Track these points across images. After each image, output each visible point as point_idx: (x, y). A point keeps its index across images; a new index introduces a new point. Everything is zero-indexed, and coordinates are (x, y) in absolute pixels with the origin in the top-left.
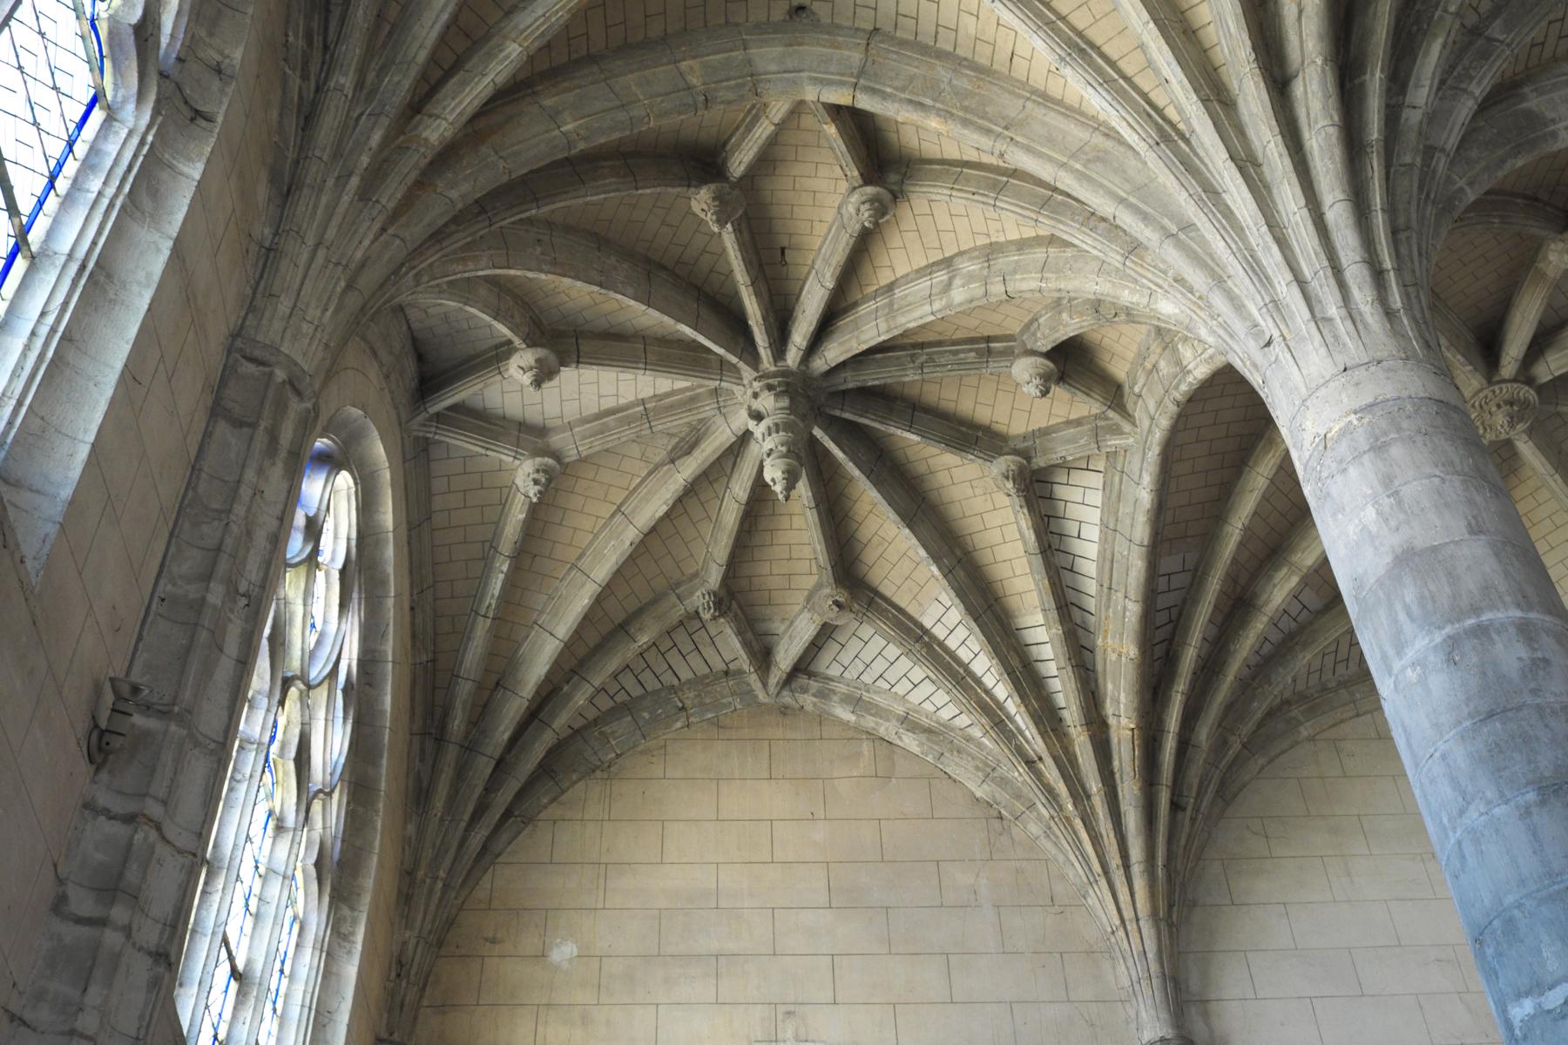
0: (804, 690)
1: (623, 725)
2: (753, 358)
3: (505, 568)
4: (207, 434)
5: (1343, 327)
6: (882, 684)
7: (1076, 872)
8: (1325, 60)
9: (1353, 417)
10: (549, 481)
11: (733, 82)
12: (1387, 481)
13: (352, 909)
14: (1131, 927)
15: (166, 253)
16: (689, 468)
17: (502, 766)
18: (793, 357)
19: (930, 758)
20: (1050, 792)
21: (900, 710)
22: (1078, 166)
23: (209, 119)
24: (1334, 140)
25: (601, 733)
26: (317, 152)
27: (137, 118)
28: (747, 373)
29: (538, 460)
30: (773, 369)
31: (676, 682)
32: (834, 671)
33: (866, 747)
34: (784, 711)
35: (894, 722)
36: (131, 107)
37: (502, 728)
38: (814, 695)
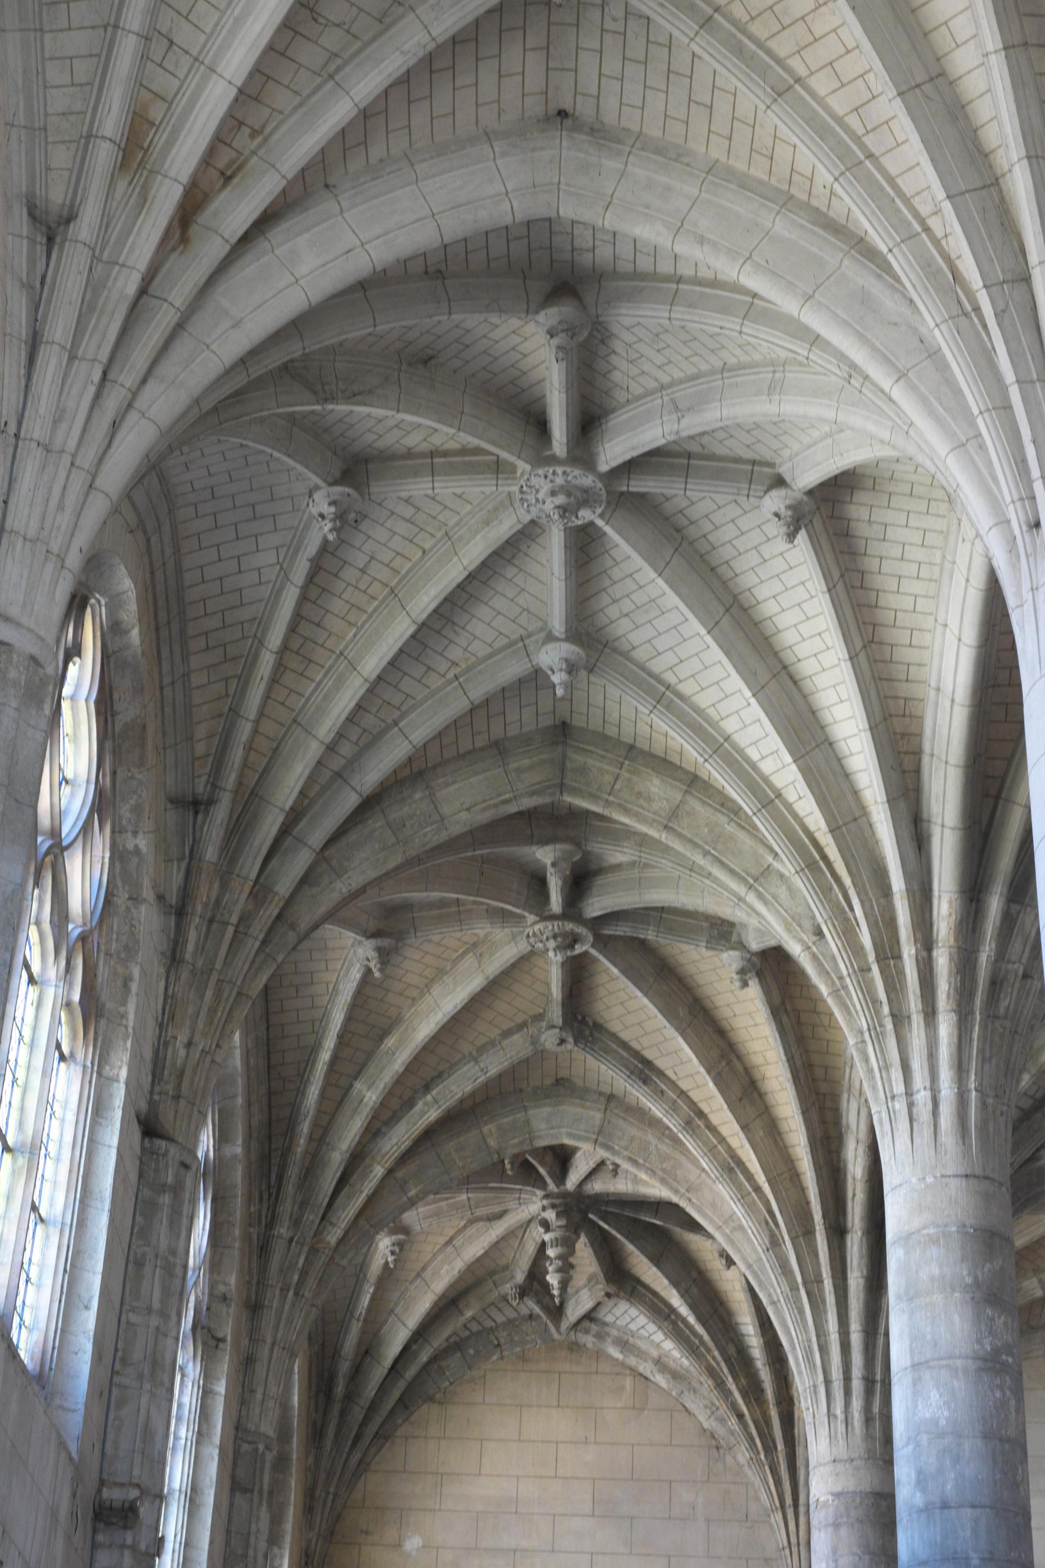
0: (587, 1331)
1: (454, 1361)
2: (543, 1185)
3: (371, 1290)
4: (231, 1505)
5: (841, 1428)
6: (642, 1331)
7: (764, 1497)
8: (863, 1233)
9: (830, 1497)
10: (401, 1250)
11: (516, 1140)
12: (835, 1551)
13: (280, 1548)
14: (795, 1549)
15: (216, 1458)
16: (498, 1229)
17: (373, 1408)
18: (572, 1182)
19: (674, 1393)
20: (752, 1439)
21: (655, 1353)
22: (727, 1231)
23: (223, 1340)
24: (861, 1288)
25: (440, 1367)
26: (270, 1282)
27: (194, 1370)
28: (540, 1193)
29: (394, 1238)
30: (556, 1190)
31: (493, 1324)
32: (609, 1319)
33: (628, 1382)
34: (574, 1347)
35: (650, 1362)
36: (191, 1365)
37: (370, 1387)
38: (594, 1336)
